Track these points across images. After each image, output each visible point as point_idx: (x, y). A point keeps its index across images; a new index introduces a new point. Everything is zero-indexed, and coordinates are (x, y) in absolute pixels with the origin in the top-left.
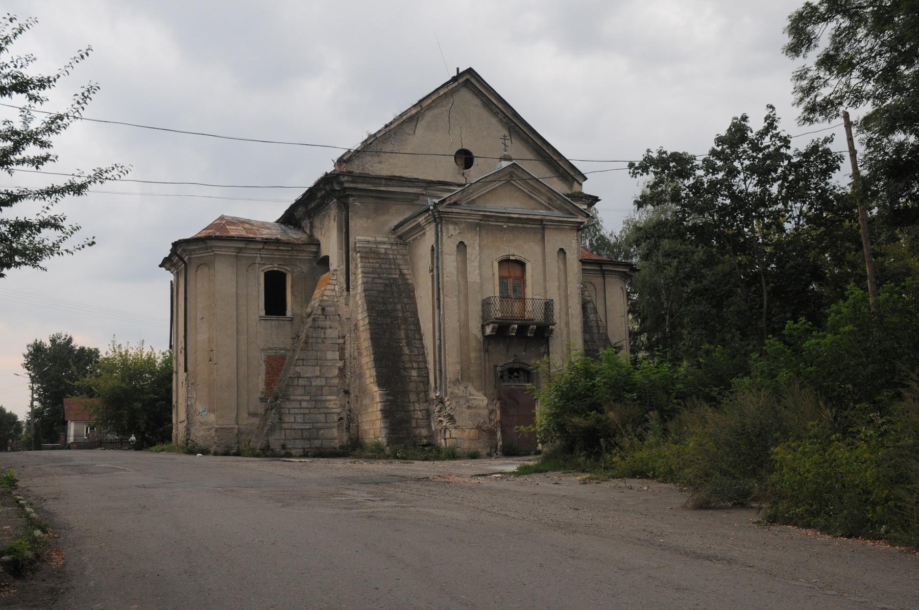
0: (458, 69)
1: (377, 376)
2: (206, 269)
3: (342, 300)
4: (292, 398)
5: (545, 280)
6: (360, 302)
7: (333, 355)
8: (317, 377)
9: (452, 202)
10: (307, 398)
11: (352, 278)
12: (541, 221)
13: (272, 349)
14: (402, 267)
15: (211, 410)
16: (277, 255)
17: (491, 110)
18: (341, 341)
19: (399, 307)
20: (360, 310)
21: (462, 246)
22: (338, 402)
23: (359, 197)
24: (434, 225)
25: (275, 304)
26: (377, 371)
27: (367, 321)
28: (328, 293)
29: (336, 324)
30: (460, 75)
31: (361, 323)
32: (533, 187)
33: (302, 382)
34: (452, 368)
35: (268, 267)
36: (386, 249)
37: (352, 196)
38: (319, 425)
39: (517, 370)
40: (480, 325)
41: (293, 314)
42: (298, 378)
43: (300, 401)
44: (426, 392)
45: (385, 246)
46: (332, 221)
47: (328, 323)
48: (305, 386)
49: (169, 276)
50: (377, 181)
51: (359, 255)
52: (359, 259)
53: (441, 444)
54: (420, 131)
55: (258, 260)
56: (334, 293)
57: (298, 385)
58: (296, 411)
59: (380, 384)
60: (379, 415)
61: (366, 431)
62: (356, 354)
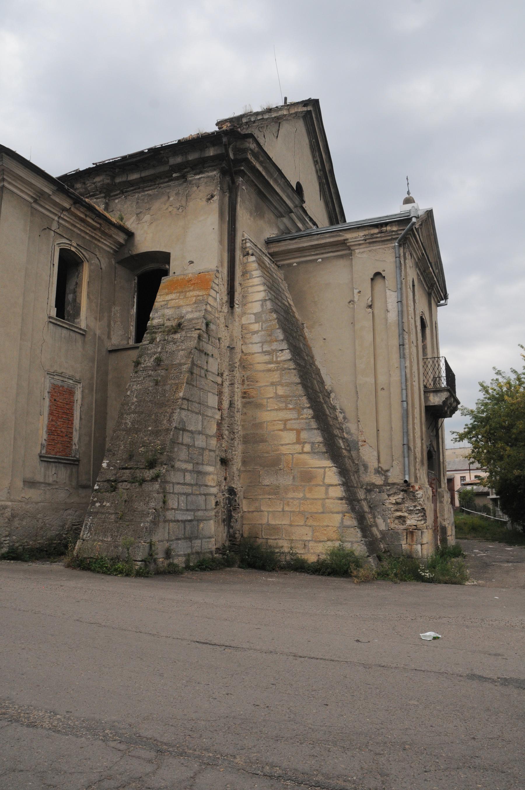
0: (286, 99)
4: (178, 464)
11: (238, 289)
17: (314, 157)
18: (219, 380)
26: (323, 437)
43: (185, 471)
48: (188, 446)
50: (272, 170)
55: (54, 226)
57: (182, 444)
61: (275, 529)
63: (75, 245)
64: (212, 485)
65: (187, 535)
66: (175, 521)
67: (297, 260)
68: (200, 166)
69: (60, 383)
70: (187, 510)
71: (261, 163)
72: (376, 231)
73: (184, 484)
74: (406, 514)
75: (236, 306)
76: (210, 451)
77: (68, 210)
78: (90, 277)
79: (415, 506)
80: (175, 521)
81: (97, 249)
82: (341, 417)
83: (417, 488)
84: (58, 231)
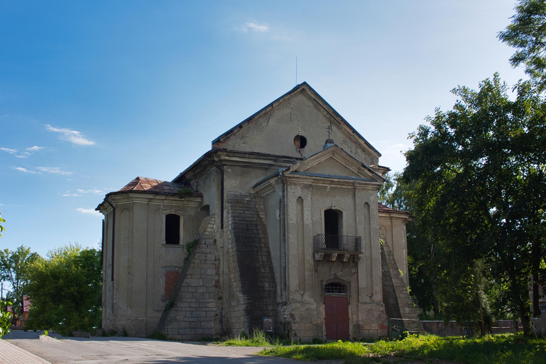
5: (356, 223)
6: (230, 237)
7: (211, 271)
8: (201, 286)
9: (294, 170)
12: (354, 183)
13: (168, 267)
16: (174, 204)
17: (319, 110)
21: (300, 200)
22: (214, 304)
23: (231, 166)
24: (281, 185)
25: (172, 237)
27: (235, 249)
28: (209, 230)
30: (298, 87)
31: (230, 251)
32: (348, 161)
33: (190, 289)
34: (294, 282)
35: (169, 212)
36: (248, 201)
37: (226, 165)
38: (202, 319)
39: (336, 284)
40: (311, 253)
43: (190, 302)
44: (275, 297)
45: (247, 199)
46: (212, 182)
47: (208, 250)
48: (193, 293)
49: (101, 216)
51: (230, 204)
52: (230, 208)
55: (162, 206)
56: (213, 230)
59: (244, 292)
62: (227, 272)
67: (265, 194)
76: (209, 293)
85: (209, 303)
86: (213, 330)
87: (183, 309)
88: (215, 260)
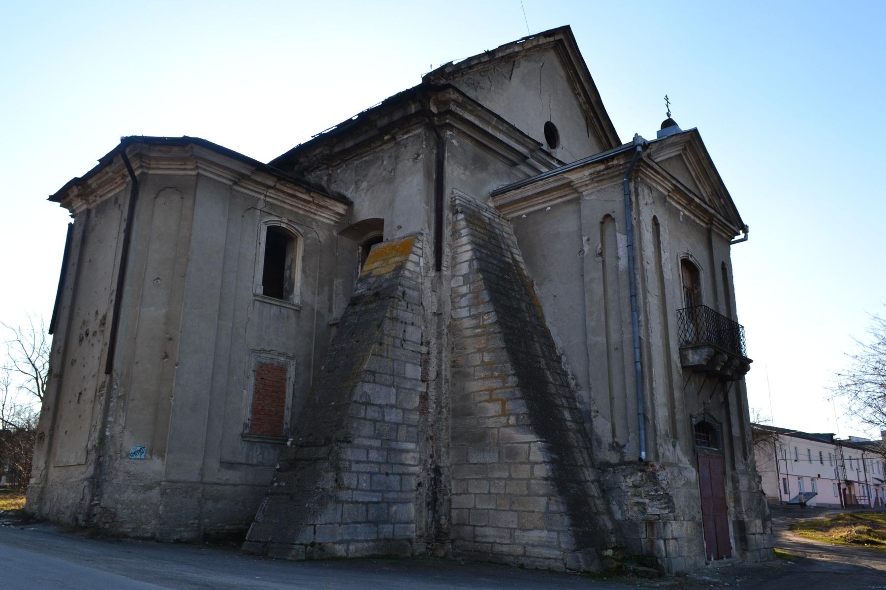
1: (530, 415)
2: (176, 198)
3: (428, 285)
4: (356, 442)
7: (413, 371)
8: (392, 406)
10: (377, 443)
11: (446, 250)
13: (264, 351)
14: (514, 251)
15: (156, 450)
17: (574, 90)
18: (424, 349)
19: (523, 305)
20: (464, 302)
29: (419, 320)
33: (372, 413)
35: (274, 220)
36: (489, 219)
37: (451, 127)
41: (302, 301)
42: (367, 404)
43: (368, 449)
46: (406, 163)
48: (374, 421)
50: (488, 117)
51: (461, 216)
52: (463, 223)
53: (659, 550)
54: (515, 80)
57: (365, 419)
58: (362, 467)
60: (541, 487)
63: (286, 221)
64: (412, 463)
65: (370, 518)
66: (352, 502)
67: (526, 211)
68: (405, 123)
69: (268, 361)
70: (372, 491)
71: (471, 112)
72: (602, 167)
73: (368, 462)
74: (647, 501)
75: (444, 269)
76: (409, 426)
77: (273, 188)
78: (305, 251)
79: (656, 491)
80: (352, 502)
81: (314, 223)
82: (573, 383)
83: (657, 467)
84: (265, 209)
85: (407, 451)
86: (413, 526)
87: (355, 468)
88: (422, 344)
